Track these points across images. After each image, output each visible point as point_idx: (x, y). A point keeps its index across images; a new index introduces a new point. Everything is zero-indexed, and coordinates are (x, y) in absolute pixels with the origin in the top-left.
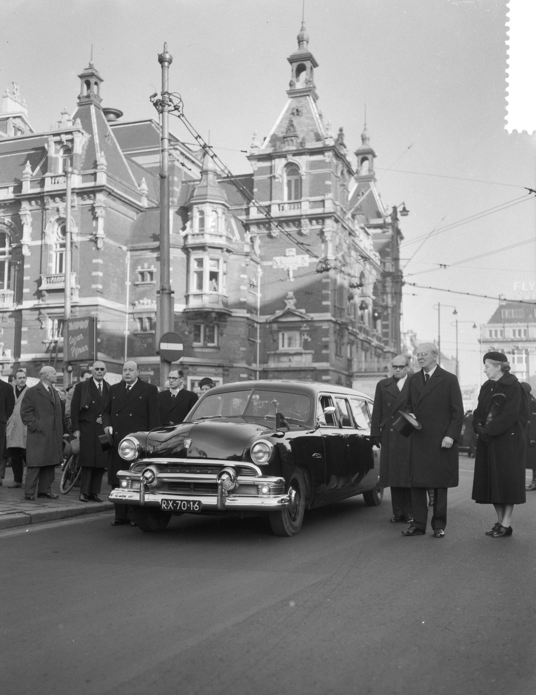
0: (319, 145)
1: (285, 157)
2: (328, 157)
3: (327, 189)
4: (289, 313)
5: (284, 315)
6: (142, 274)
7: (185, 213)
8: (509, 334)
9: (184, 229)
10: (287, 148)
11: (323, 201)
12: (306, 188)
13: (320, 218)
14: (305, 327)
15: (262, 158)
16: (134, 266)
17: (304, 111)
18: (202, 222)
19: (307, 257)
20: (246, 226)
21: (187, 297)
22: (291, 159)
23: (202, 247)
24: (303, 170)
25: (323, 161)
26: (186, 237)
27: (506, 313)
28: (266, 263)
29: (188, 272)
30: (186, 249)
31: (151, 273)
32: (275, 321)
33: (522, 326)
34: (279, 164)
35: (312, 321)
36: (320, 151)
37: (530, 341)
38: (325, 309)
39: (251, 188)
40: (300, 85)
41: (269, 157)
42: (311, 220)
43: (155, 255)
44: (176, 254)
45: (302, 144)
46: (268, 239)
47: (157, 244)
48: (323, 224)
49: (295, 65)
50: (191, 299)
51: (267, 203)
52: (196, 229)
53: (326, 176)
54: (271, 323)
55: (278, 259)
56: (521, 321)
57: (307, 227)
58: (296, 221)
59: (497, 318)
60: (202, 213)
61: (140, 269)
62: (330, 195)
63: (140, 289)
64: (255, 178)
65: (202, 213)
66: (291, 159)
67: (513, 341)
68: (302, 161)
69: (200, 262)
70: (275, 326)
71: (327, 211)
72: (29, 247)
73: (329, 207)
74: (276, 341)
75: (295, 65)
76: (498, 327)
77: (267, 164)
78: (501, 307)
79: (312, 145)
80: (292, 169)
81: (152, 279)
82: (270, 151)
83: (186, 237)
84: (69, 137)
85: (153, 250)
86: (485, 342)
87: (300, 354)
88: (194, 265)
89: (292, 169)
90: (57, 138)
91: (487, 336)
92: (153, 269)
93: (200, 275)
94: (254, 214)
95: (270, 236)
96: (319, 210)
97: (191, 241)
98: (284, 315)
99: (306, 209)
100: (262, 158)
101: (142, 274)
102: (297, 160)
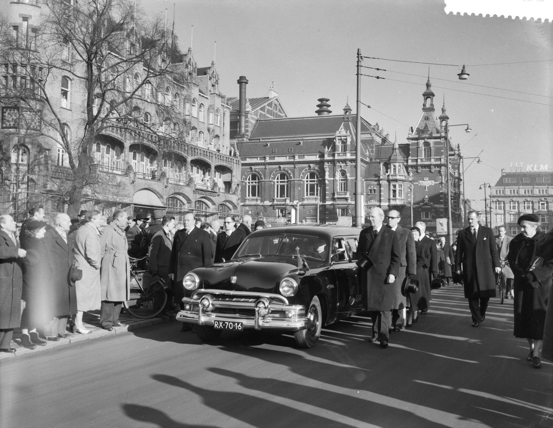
0: (438, 135)
1: (424, 139)
2: (442, 140)
3: (441, 154)
4: (426, 204)
5: (424, 205)
6: (371, 190)
7: (387, 166)
8: (508, 192)
9: (387, 172)
10: (424, 136)
11: (440, 159)
12: (433, 153)
13: (439, 166)
14: (433, 210)
15: (413, 139)
16: (367, 187)
17: (430, 118)
18: (395, 169)
19: (433, 181)
20: (407, 167)
21: (389, 200)
22: (426, 140)
23: (396, 180)
24: (432, 145)
25: (440, 142)
26: (388, 176)
27: (506, 180)
28: (415, 183)
29: (389, 189)
30: (389, 181)
31: (375, 190)
32: (420, 207)
33: (516, 188)
34: (421, 142)
35: (436, 208)
36: (439, 138)
37: (520, 197)
38: (441, 203)
39: (409, 151)
40: (428, 106)
41: (416, 139)
42: (435, 167)
43: (376, 183)
44: (384, 183)
45: (431, 134)
46: (416, 173)
47: (377, 178)
48: (440, 168)
49: (426, 97)
50: (391, 200)
51: (416, 158)
52: (392, 173)
53: (441, 148)
54: (418, 208)
55: (421, 182)
56: (515, 185)
57: (433, 169)
58: (429, 166)
59: (500, 183)
60: (395, 166)
61: (369, 188)
62: (443, 156)
63: (370, 196)
64: (411, 147)
65: (395, 166)
66: (426, 140)
67: (509, 197)
68: (431, 141)
69: (395, 186)
70: (420, 209)
71: (442, 163)
72: (328, 180)
73: (443, 161)
74: (420, 215)
75: (426, 97)
76: (501, 188)
77: (416, 142)
78: (503, 177)
79: (435, 135)
80: (427, 144)
81: (375, 192)
82: (417, 136)
83: (388, 176)
84: (345, 138)
85: (375, 181)
86: (494, 197)
87: (431, 221)
88: (392, 188)
89: (427, 144)
90: (340, 138)
91: (495, 194)
92: (375, 188)
93: (394, 191)
94: (410, 163)
95: (417, 172)
96: (439, 163)
97: (391, 178)
98: (424, 205)
99: (433, 162)
100: (413, 139)
101: (371, 190)
102: (429, 140)
